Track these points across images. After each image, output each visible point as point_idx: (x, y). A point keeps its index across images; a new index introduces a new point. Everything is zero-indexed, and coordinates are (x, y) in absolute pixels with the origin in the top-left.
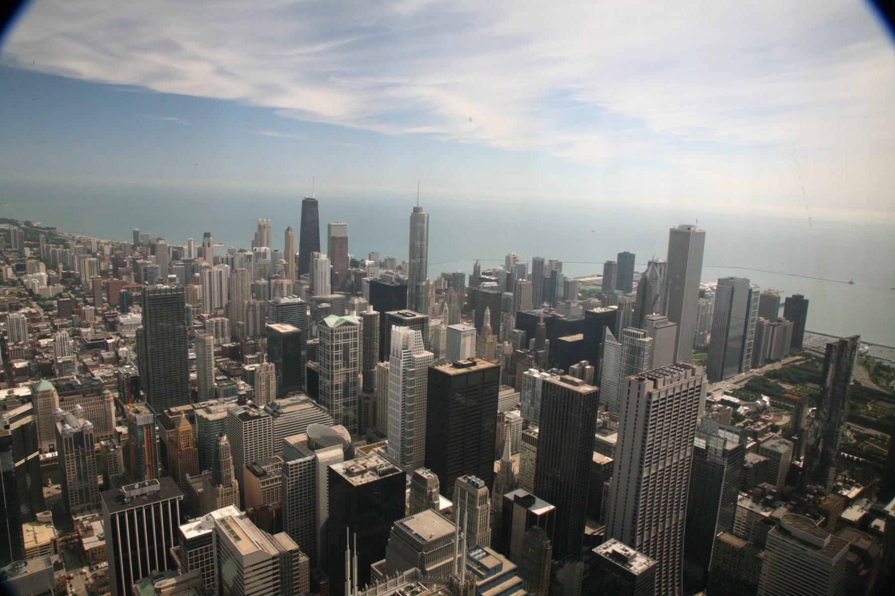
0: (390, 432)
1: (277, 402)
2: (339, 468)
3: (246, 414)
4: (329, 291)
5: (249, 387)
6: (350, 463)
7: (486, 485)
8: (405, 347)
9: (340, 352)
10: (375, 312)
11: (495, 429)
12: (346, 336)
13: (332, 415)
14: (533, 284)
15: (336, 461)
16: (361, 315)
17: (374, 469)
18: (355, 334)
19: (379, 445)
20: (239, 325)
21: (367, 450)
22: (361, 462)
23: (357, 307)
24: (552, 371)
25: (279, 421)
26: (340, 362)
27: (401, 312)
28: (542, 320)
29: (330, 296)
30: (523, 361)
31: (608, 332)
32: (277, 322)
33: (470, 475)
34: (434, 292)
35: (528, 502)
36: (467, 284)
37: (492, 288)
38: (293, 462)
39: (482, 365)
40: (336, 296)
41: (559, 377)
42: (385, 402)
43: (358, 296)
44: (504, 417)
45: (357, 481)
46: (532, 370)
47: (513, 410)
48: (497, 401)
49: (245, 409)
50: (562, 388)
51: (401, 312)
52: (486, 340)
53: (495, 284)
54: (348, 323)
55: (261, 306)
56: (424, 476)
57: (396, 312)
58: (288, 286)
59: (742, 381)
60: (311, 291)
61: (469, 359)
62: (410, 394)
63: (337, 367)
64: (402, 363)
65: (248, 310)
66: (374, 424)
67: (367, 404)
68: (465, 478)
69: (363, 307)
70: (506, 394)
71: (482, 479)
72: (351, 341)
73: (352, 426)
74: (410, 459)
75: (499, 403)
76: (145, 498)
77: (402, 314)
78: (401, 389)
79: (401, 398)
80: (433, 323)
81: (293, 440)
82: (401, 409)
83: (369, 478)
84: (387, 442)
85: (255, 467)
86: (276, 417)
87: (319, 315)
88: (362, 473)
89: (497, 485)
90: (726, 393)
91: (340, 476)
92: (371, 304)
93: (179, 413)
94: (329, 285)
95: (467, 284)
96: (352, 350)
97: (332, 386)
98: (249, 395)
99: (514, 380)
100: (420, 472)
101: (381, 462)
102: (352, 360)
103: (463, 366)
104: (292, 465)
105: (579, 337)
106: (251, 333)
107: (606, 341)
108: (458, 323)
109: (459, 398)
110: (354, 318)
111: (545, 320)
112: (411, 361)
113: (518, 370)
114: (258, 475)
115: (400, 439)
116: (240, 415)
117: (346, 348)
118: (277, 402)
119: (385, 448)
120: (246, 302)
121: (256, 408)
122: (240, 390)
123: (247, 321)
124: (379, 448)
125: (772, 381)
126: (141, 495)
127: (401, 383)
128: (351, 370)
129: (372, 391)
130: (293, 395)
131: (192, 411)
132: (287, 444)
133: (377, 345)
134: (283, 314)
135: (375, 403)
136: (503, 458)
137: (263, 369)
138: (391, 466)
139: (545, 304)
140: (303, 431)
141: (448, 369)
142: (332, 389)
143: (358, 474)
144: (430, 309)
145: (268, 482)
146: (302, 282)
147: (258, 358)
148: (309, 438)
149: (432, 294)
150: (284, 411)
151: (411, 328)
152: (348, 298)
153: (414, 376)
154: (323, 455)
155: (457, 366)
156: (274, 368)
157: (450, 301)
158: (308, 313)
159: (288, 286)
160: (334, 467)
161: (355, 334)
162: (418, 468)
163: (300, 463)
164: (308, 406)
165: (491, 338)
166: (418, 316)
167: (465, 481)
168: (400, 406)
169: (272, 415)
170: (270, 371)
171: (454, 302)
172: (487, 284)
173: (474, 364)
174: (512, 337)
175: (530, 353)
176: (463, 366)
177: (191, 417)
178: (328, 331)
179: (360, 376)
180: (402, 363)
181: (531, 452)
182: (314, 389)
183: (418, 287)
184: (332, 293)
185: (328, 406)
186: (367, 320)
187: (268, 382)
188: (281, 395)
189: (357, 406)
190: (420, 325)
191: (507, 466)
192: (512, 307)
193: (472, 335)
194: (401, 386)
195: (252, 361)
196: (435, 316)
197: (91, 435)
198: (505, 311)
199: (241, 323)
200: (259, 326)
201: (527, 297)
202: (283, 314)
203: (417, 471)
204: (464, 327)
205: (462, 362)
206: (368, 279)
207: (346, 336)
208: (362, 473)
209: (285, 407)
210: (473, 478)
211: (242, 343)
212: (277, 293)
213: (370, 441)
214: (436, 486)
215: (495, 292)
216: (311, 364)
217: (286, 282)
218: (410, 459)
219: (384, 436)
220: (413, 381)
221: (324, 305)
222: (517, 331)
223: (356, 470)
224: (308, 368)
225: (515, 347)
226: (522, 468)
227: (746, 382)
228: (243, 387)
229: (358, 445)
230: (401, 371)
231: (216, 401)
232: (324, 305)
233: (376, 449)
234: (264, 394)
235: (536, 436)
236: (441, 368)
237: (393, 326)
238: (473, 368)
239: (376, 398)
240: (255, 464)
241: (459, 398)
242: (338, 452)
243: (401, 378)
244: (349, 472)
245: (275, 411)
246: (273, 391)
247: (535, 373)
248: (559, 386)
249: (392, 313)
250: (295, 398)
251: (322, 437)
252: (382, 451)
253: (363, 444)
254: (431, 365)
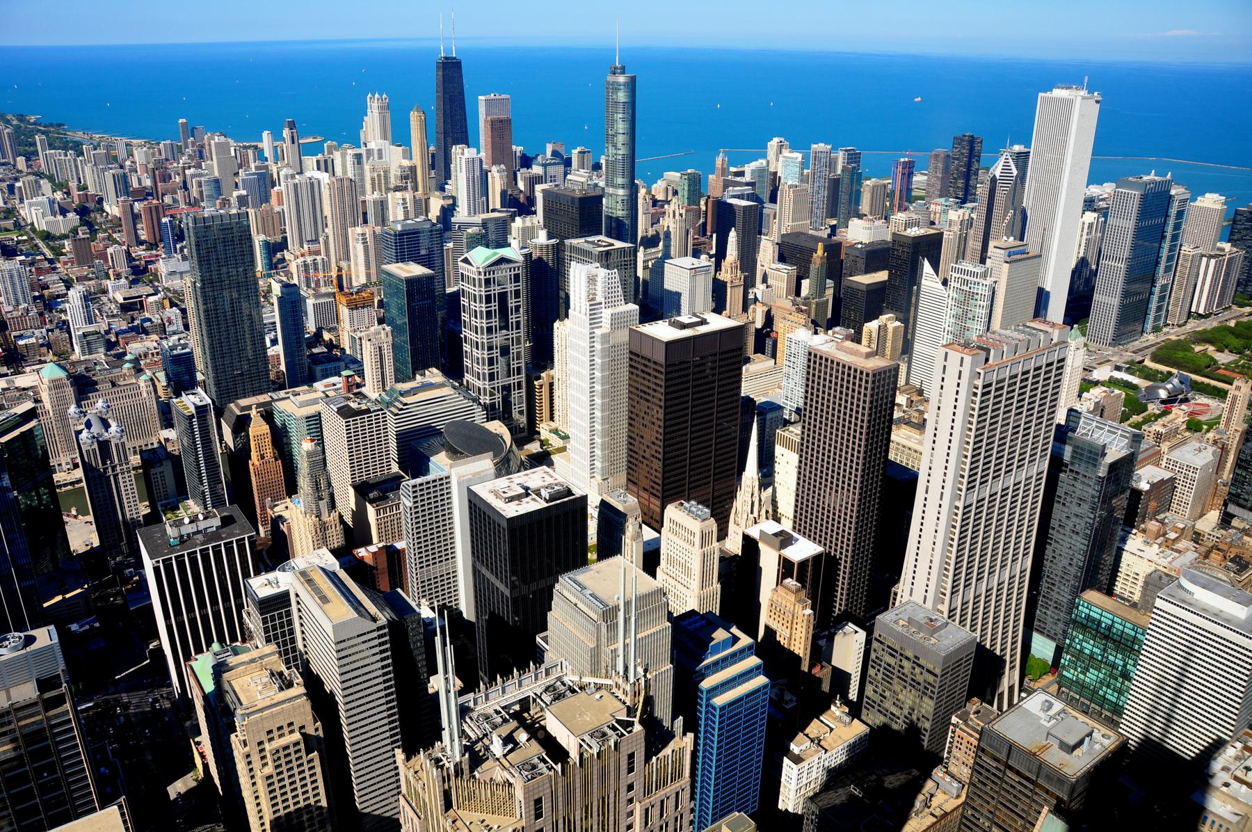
6: (502, 482)
22: (520, 481)
31: (927, 267)
35: (784, 540)
39: (717, 323)
48: (740, 381)
54: (503, 260)
57: (582, 240)
59: (1147, 348)
66: (552, 419)
71: (708, 507)
75: (743, 384)
76: (200, 537)
77: (593, 243)
90: (1118, 368)
93: (249, 408)
96: (512, 303)
102: (512, 319)
103: (684, 326)
105: (882, 276)
107: (923, 282)
125: (1198, 348)
126: (194, 533)
128: (513, 334)
131: (269, 403)
164: (447, 391)
173: (704, 322)
177: (268, 416)
197: (123, 444)
205: (684, 318)
227: (1153, 349)
231: (306, 387)
238: (702, 330)
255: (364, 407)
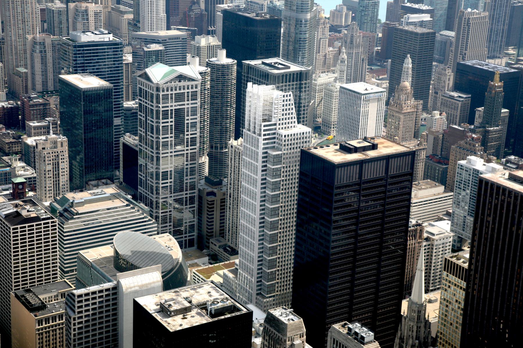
0: (242, 248)
1: (70, 196)
2: (150, 304)
3: (18, 214)
4: (164, 25)
5: (30, 172)
6: (168, 295)
7: (376, 338)
8: (267, 118)
9: (171, 122)
10: (230, 61)
11: (405, 249)
12: (179, 97)
13: (157, 218)
14: (492, 17)
15: (148, 291)
16: (208, 65)
17: (203, 306)
18: (194, 96)
19: (226, 266)
20: (19, 74)
21: (208, 273)
22: (185, 294)
23: (204, 53)
24: (508, 161)
25: (70, 226)
26: (170, 138)
27: (268, 61)
28: (497, 77)
29: (164, 33)
30: (462, 142)
32: (76, 72)
33: (351, 322)
34: (327, 30)
36: (382, 15)
37: (422, 24)
38: (82, 291)
39: (387, 148)
40: (173, 33)
41: (507, 173)
42: (237, 201)
43: (208, 33)
44: (421, 231)
45: (174, 324)
46: (472, 158)
47: (441, 219)
48: (408, 207)
49: (16, 206)
50: (511, 191)
51: (268, 61)
52: (401, 108)
53: (427, 17)
54: (181, 77)
55: (53, 46)
56: (283, 319)
57: (259, 62)
58: (96, 14)
60: (135, 25)
61: (365, 139)
62: (273, 190)
63: (165, 145)
64: (261, 142)
65: (33, 51)
66: (222, 233)
67: (212, 203)
68: (343, 326)
69: (212, 51)
70: (425, 194)
71: (371, 329)
72: (187, 105)
73: (186, 237)
74: (271, 289)
75: (413, 209)
78: (259, 182)
79: (259, 195)
80: (322, 79)
81: (92, 255)
82: (258, 212)
83: (195, 319)
84: (237, 261)
85: (28, 296)
86: (68, 219)
87: (144, 60)
88: (184, 311)
89: (402, 339)
91: (150, 315)
92: (224, 46)
94: (163, 15)
95: (382, 15)
96: (188, 120)
97: (157, 174)
98: (31, 184)
99: (445, 172)
100: (277, 312)
101: (216, 295)
102: (188, 135)
103: (356, 150)
104: (80, 296)
106: (39, 87)
108: (362, 79)
109: (351, 197)
110: (194, 69)
111: (504, 77)
112: (273, 139)
113: (451, 157)
114: (32, 309)
115: (256, 259)
116: (7, 216)
117: (179, 114)
118: (70, 196)
119: (235, 272)
120: (30, 37)
121: (34, 204)
122: (16, 176)
123: (33, 67)
124: (226, 271)
127: (260, 173)
129: (220, 183)
130: (97, 186)
132: (83, 261)
133: (232, 112)
134: (86, 58)
135: (223, 201)
136: (414, 296)
137: (48, 145)
138: (229, 303)
139: (511, 51)
140: (109, 242)
141: (332, 155)
142: (158, 178)
143: (177, 312)
144: (320, 57)
145: (47, 320)
146: (122, 8)
147: (44, 127)
148: (116, 252)
149: (322, 34)
150: (81, 210)
151: (278, 88)
152: (193, 35)
153: (280, 162)
154: (129, 282)
155: (345, 149)
156: (66, 144)
157: (350, 43)
158: (129, 58)
159: (96, 14)
160: (141, 301)
161: (194, 96)
162: (276, 305)
163: (94, 293)
164: (118, 203)
165: (410, 104)
166: (294, 68)
167: (345, 331)
168: (258, 208)
169: (61, 215)
170: (59, 149)
171: (358, 46)
172: (414, 18)
173: (374, 147)
174: (446, 105)
175: (473, 131)
176: (356, 150)
178: (151, 88)
179: (205, 159)
180: (261, 142)
181: (457, 290)
182: (131, 177)
183: (298, 22)
184: (168, 28)
185: (150, 204)
186: (218, 72)
187: (56, 166)
188: (77, 185)
189: (196, 205)
190: (298, 82)
191: (419, 310)
192: (451, 56)
193: (379, 100)
194: (259, 177)
195: (39, 131)
196: (327, 67)
198: (440, 62)
199: (22, 70)
200: (50, 76)
201: (478, 39)
202: (86, 58)
203: (272, 311)
204: (371, 87)
205: (355, 143)
206: (225, 6)
207: (179, 97)
208: (184, 311)
209: (82, 204)
210: (356, 327)
211: (23, 103)
212: (79, 26)
213: (214, 258)
214: (301, 336)
215: (425, 30)
216: (130, 139)
217: (92, 7)
218: (271, 289)
219: (234, 252)
220: (279, 170)
221: (155, 47)
222: (455, 94)
223: (175, 307)
224: (126, 146)
225: (450, 120)
226: (443, 316)
228: (22, 172)
229: (192, 266)
230: (261, 155)
232: (155, 47)
233: (221, 272)
234: (49, 183)
235: (466, 266)
236: (321, 152)
237: (250, 84)
238: (372, 154)
239: (224, 194)
240: (28, 291)
241: (351, 197)
242: (153, 277)
243: (260, 164)
244: (164, 310)
245: (66, 210)
246: (64, 179)
247: (477, 163)
248: (505, 189)
249: (253, 63)
250: (98, 190)
251: (134, 253)
252: (231, 275)
253: (203, 263)
254: (305, 146)
255: (33, 215)
